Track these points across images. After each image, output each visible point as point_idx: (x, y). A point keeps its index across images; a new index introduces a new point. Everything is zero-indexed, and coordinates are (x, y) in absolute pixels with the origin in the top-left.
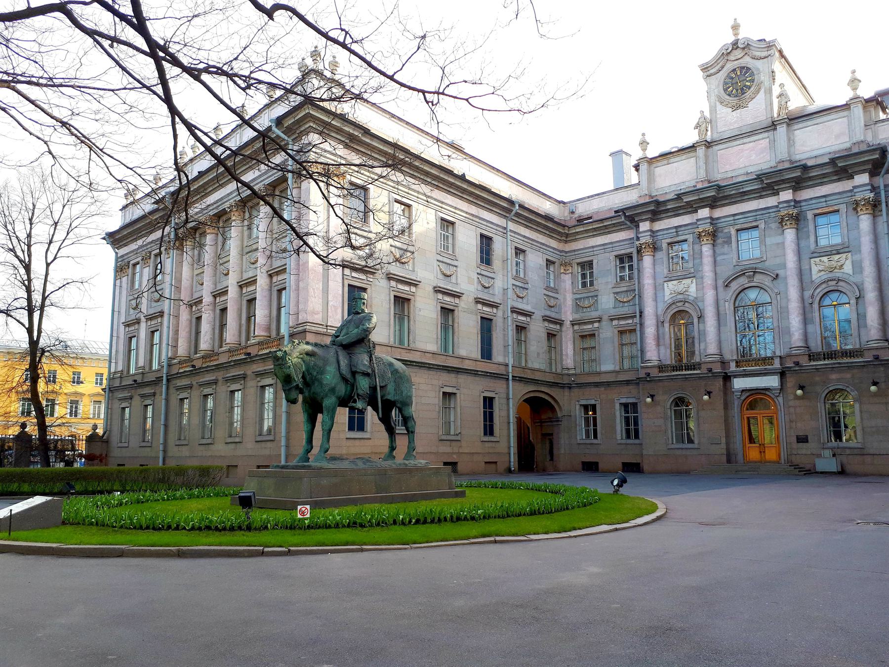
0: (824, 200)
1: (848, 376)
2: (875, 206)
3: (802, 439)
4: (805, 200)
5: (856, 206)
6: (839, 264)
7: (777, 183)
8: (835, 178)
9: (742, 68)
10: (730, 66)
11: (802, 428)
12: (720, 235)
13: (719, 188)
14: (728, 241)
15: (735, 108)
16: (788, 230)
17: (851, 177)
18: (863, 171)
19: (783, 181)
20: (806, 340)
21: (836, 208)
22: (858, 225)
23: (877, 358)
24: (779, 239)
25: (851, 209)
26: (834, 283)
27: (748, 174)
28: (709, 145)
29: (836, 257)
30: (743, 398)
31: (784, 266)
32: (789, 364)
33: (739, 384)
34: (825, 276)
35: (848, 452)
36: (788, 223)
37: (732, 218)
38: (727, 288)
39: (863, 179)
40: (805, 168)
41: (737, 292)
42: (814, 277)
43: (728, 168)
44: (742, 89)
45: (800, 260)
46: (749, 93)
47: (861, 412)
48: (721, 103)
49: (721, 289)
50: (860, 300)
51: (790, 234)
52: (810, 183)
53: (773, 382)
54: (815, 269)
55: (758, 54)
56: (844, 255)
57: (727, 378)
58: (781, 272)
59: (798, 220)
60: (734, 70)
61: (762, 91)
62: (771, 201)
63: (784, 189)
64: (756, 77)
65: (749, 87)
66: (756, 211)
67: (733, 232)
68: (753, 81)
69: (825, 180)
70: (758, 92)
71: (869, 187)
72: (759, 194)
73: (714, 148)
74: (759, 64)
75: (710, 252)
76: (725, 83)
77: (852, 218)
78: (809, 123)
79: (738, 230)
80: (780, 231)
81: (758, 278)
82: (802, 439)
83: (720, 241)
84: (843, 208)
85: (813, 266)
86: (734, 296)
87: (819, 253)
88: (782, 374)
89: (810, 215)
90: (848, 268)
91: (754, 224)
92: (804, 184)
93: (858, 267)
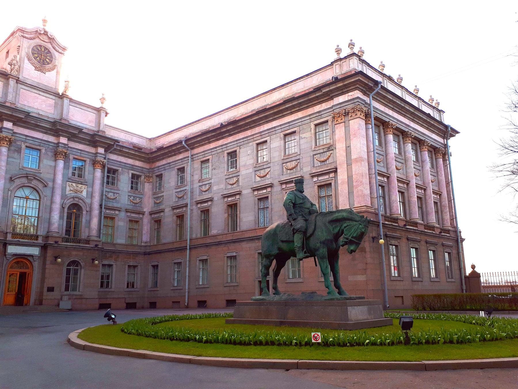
0: (80, 152)
1: (81, 254)
2: (104, 166)
3: (51, 289)
4: (71, 148)
7: (63, 131)
9: (46, 48)
10: (37, 41)
11: (49, 283)
12: (13, 144)
13: (27, 114)
14: (19, 151)
15: (36, 69)
16: (61, 161)
17: (96, 147)
19: (66, 132)
20: (59, 228)
21: (85, 159)
22: (94, 173)
23: (96, 246)
24: (52, 163)
25: (91, 162)
26: (77, 199)
27: (39, 114)
28: (18, 81)
29: (80, 186)
30: (10, 260)
31: (54, 181)
32: (51, 241)
33: (12, 250)
34: (73, 195)
35: (74, 297)
36: (62, 157)
37: (25, 137)
38: (12, 182)
39: (101, 150)
41: (19, 186)
42: (67, 193)
43: (26, 103)
44: (43, 61)
45: (63, 181)
46: (47, 67)
47: (84, 274)
48: (29, 60)
49: (8, 181)
50: (89, 213)
51: (61, 164)
53: (35, 251)
54: (68, 188)
55: (57, 48)
56: (84, 186)
57: (5, 245)
58: (50, 184)
59: (66, 157)
60: (40, 46)
61: (55, 71)
62: (52, 139)
64: (53, 60)
65: (48, 64)
66: (42, 140)
67: (23, 146)
68: (51, 61)
70: (53, 70)
71: (104, 156)
72: (46, 131)
73: (19, 85)
74: (56, 54)
75: (6, 154)
76: (33, 49)
79: (26, 147)
80: (53, 159)
81: (34, 183)
82: (51, 289)
83: (12, 148)
84: (88, 161)
85: (67, 186)
86: (16, 188)
87: (70, 180)
88: (44, 248)
89: (71, 157)
90: (84, 194)
91: (38, 147)
92: (72, 138)
93: (91, 195)
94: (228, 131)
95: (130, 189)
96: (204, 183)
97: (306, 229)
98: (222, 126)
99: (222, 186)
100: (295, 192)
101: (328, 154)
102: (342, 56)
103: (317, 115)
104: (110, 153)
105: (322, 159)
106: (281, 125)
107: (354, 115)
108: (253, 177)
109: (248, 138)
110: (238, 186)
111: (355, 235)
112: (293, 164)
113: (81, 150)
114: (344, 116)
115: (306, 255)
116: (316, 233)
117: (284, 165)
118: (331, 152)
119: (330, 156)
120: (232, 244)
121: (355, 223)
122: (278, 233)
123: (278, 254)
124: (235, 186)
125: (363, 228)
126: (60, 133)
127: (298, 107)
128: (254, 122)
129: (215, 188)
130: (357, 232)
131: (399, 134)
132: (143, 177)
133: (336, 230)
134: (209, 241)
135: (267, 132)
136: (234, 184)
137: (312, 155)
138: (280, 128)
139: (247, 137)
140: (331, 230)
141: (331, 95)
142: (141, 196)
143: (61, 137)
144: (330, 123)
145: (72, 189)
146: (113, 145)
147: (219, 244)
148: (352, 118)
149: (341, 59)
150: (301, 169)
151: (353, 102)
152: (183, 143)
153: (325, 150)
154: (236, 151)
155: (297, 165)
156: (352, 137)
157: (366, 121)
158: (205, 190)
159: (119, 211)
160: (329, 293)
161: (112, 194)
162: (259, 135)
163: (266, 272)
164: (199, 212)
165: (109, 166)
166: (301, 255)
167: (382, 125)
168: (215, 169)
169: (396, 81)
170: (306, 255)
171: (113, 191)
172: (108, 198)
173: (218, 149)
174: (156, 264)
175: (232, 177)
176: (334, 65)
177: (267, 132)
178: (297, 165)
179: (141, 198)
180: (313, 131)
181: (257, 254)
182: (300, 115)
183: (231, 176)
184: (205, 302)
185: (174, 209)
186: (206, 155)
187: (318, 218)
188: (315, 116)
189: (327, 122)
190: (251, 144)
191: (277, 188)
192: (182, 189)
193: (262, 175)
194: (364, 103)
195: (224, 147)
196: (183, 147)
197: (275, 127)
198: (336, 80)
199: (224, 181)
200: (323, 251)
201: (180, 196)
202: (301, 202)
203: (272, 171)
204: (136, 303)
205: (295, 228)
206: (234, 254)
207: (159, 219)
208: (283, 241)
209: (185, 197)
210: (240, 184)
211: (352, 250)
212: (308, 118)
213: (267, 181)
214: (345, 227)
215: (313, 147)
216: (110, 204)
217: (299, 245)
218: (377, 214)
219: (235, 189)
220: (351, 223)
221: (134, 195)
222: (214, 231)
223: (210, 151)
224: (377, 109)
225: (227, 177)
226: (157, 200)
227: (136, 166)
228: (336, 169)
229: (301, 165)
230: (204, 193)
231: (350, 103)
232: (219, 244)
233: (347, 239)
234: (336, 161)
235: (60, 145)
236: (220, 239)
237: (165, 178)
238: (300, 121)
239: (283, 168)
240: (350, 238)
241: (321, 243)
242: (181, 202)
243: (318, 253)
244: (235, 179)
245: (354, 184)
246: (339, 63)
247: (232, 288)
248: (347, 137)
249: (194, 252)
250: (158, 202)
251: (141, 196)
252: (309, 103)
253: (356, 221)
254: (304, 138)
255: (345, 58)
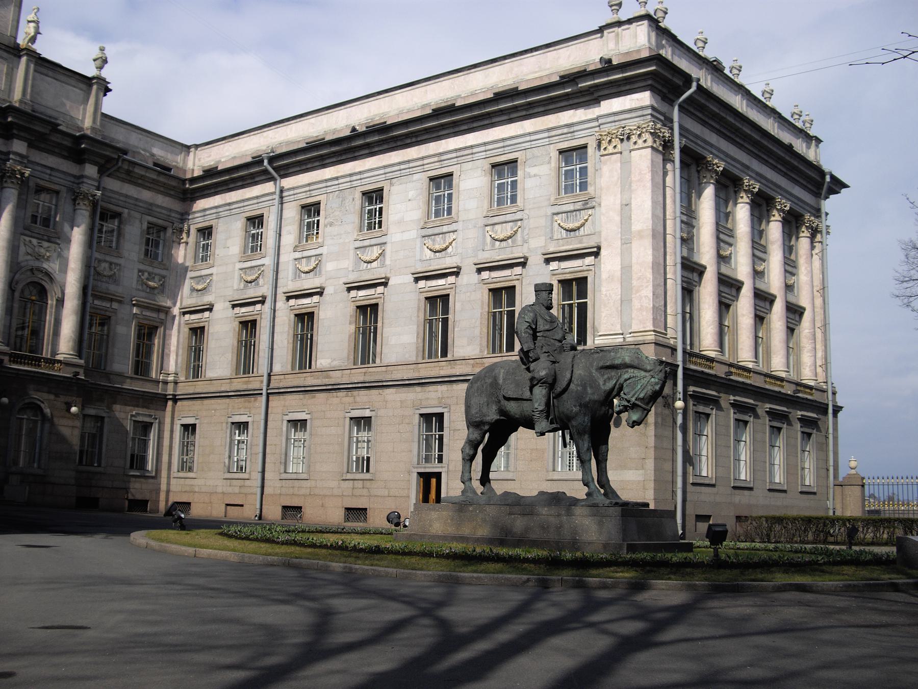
0: (48, 171)
2: (94, 204)
5: (76, 197)
6: (48, 254)
7: (21, 128)
8: (66, 154)
18: (95, 163)
21: (57, 187)
29: (46, 244)
39: (91, 170)
40: (54, 127)
42: (21, 258)
52: (43, 146)
54: (22, 249)
56: (53, 245)
63: (20, 138)
69: (56, 150)
77: (68, 208)
78: (50, 73)
84: (64, 189)
85: (22, 245)
94: (368, 146)
95: (142, 257)
96: (306, 254)
97: (555, 380)
98: (355, 134)
99: (347, 263)
100: (536, 308)
101: (584, 214)
102: (623, 15)
103: (565, 130)
104: (108, 176)
105: (571, 226)
106: (485, 144)
107: (640, 142)
108: (418, 249)
109: (411, 165)
110: (383, 265)
111: (642, 396)
112: (507, 230)
113: (52, 169)
114: (622, 140)
115: (554, 426)
116: (572, 386)
117: (488, 228)
118: (590, 212)
119: (586, 220)
120: (363, 392)
121: (643, 373)
122: (501, 382)
123: (497, 421)
124: (374, 264)
125: (656, 384)
126: (15, 131)
127: (525, 110)
128: (427, 130)
129: (329, 267)
130: (645, 391)
131: (728, 183)
132: (170, 231)
133: (610, 385)
134: (310, 380)
135: (454, 155)
136: (374, 260)
137: (549, 213)
138: (483, 148)
139: (409, 161)
140: (601, 383)
141: (596, 95)
142: (164, 272)
143: (15, 141)
144: (591, 150)
145: (29, 251)
146: (118, 160)
147: (334, 389)
148: (636, 147)
149: (619, 24)
150: (525, 241)
151: (640, 113)
152: (266, 162)
153: (579, 206)
154: (381, 190)
155: (516, 232)
156: (634, 186)
157: (664, 155)
158: (306, 269)
159: (120, 302)
160: (588, 494)
161: (106, 265)
162: (436, 159)
163: (472, 452)
164: (293, 316)
165: (104, 204)
166: (543, 424)
167: (693, 163)
168: (331, 224)
169: (727, 71)
170: (554, 426)
171: (108, 258)
172: (99, 274)
173: (341, 181)
174: (190, 421)
175: (371, 246)
176: (606, 32)
177: (454, 155)
178: (516, 232)
179: (164, 277)
180: (554, 164)
181: (417, 416)
182: (529, 125)
183: (367, 243)
184: (299, 509)
185: (234, 306)
186: (314, 193)
187: (577, 361)
188: (560, 132)
189: (584, 147)
190: (416, 177)
191: (468, 277)
192: (254, 263)
193: (437, 247)
194: (662, 118)
195: (354, 178)
196: (266, 172)
197: (472, 147)
198: (608, 66)
199: (352, 252)
200: (584, 420)
201: (249, 279)
202: (547, 327)
203: (459, 240)
204: (147, 501)
205: (536, 375)
206: (367, 413)
207: (202, 325)
208: (508, 399)
209: (261, 281)
210: (388, 262)
211: (634, 422)
212: (546, 135)
213: (448, 262)
214: (626, 380)
215: (553, 199)
216: (103, 286)
217: (541, 408)
218: (674, 350)
219: (374, 272)
220: (637, 373)
221: (150, 269)
222: (322, 361)
223: (324, 185)
224: (687, 130)
225: (359, 244)
226: (198, 284)
227: (158, 206)
228: (599, 248)
229: (526, 232)
230: (303, 275)
231: (633, 115)
232: (334, 389)
233: (629, 401)
234: (600, 232)
235: (11, 156)
236: (336, 378)
237: (219, 236)
238: (528, 138)
239: (485, 236)
240: (633, 399)
241: (580, 405)
242: (253, 292)
243: (574, 423)
244: (376, 252)
245: (635, 283)
246: (616, 29)
247: (359, 484)
248: (626, 183)
249: (275, 402)
250: (200, 287)
251: (164, 272)
252: (549, 104)
253: (646, 371)
254: (535, 176)
255: (630, 21)
